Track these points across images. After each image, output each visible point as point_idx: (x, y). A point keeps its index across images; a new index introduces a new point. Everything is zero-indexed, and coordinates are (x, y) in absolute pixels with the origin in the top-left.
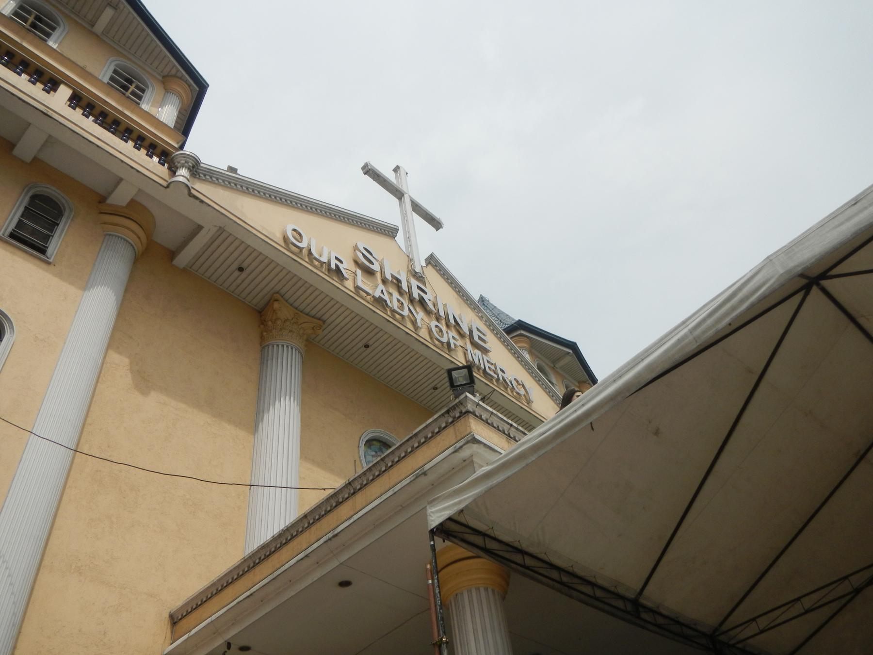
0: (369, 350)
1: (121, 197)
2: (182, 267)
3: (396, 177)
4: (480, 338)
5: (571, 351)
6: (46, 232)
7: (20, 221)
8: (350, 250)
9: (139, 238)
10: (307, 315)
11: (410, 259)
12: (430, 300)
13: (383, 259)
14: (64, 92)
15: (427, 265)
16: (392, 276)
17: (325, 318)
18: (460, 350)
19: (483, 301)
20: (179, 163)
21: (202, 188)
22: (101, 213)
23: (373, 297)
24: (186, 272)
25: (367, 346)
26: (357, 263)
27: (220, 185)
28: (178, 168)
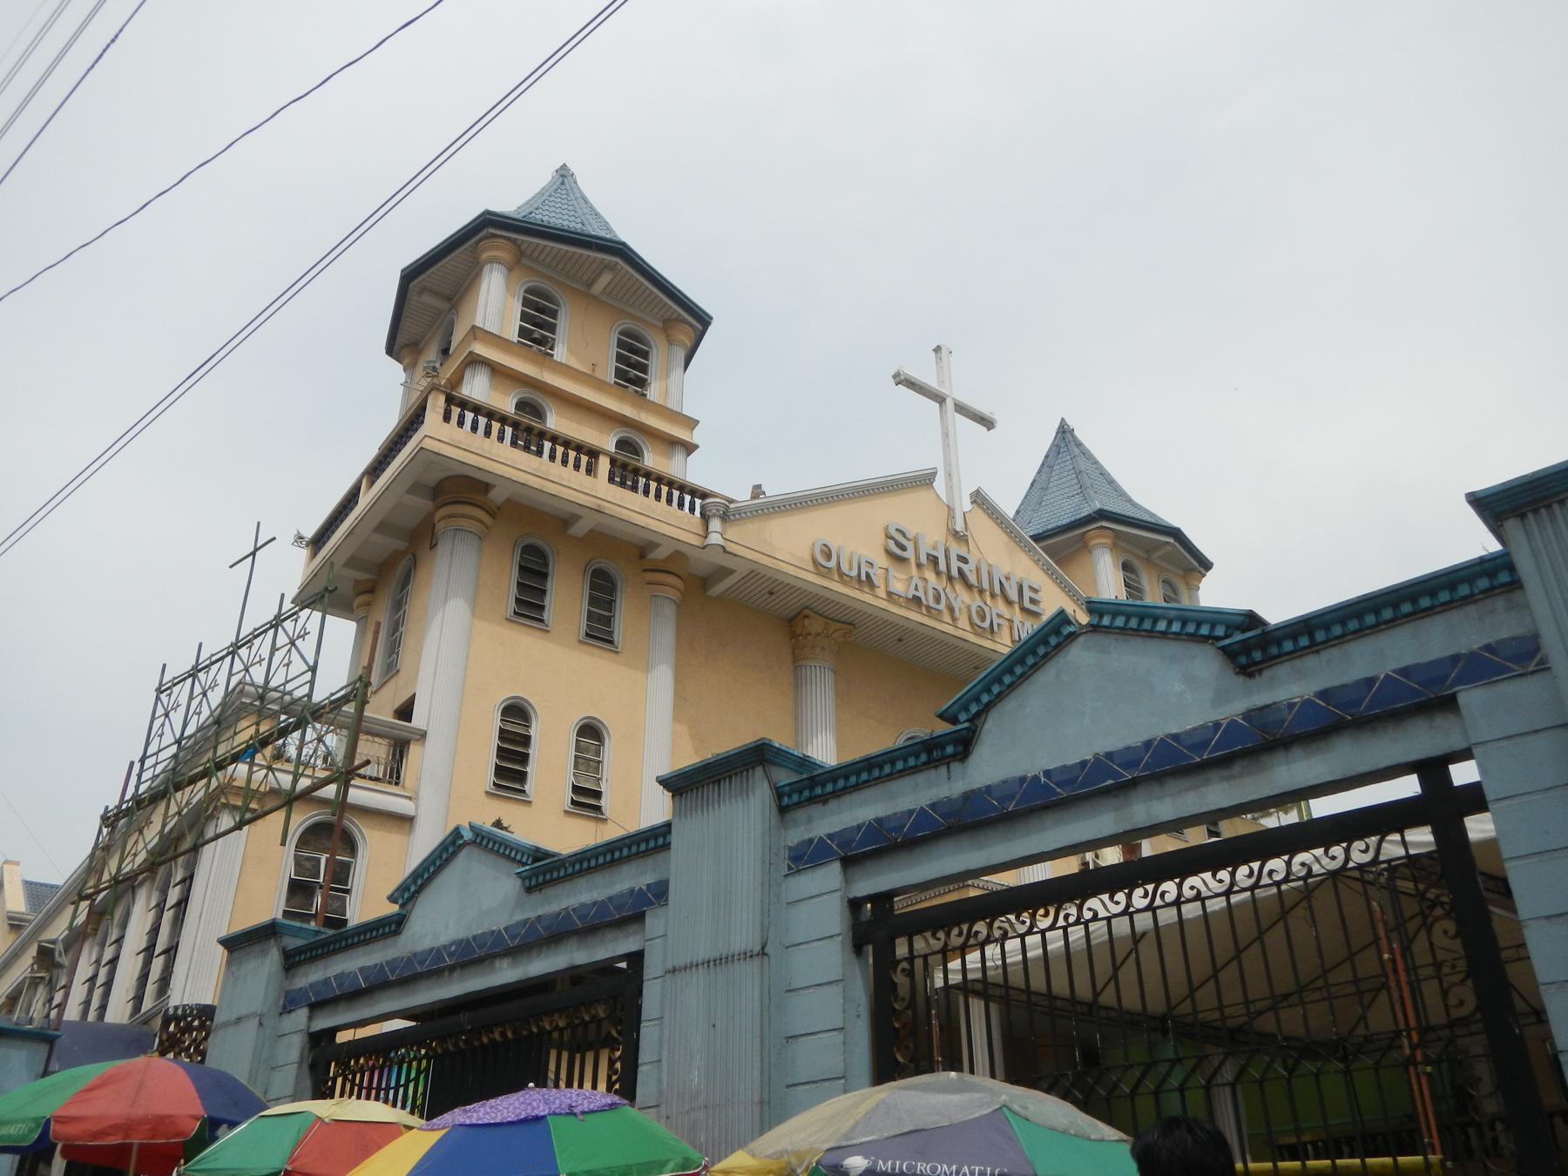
0: (902, 643)
1: (659, 554)
2: (714, 595)
3: (940, 368)
4: (1032, 601)
5: (1172, 540)
6: (607, 614)
7: (589, 610)
8: (880, 538)
9: (678, 590)
10: (836, 621)
11: (950, 509)
12: (970, 571)
13: (917, 534)
15: (972, 503)
16: (928, 555)
17: (855, 622)
18: (1006, 631)
19: (1064, 432)
20: (710, 511)
21: (734, 533)
22: (646, 571)
23: (908, 599)
24: (720, 598)
25: (900, 640)
26: (889, 553)
27: (748, 517)
28: (709, 517)
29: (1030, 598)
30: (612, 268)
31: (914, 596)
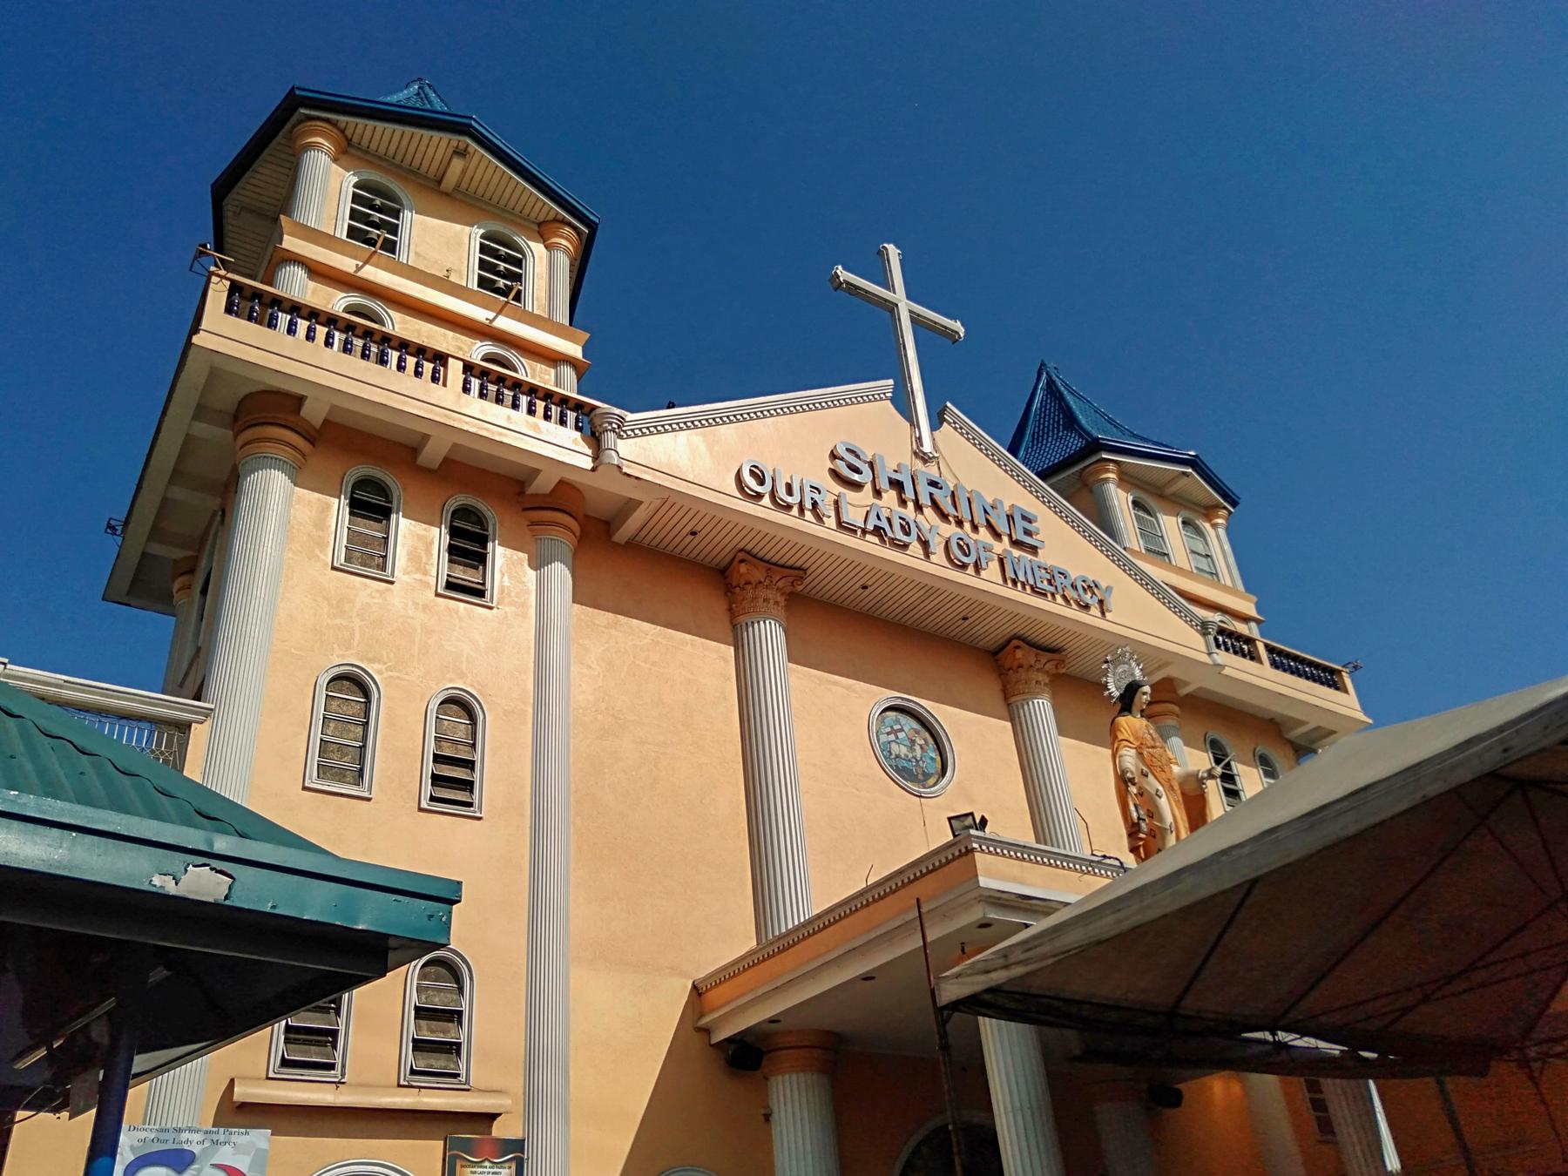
1: (544, 484)
4: (1028, 533)
14: (455, 369)
17: (805, 566)
22: (525, 509)
29: (1024, 528)
30: (461, 153)
31: (875, 526)
